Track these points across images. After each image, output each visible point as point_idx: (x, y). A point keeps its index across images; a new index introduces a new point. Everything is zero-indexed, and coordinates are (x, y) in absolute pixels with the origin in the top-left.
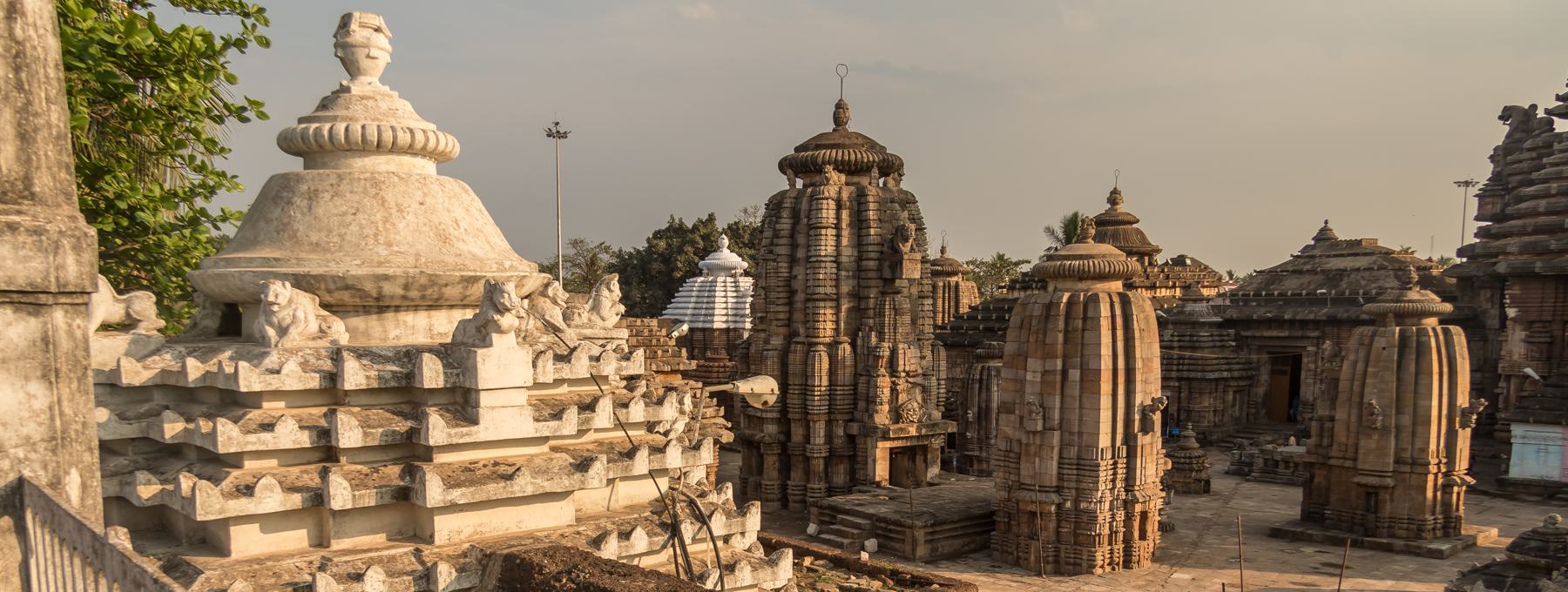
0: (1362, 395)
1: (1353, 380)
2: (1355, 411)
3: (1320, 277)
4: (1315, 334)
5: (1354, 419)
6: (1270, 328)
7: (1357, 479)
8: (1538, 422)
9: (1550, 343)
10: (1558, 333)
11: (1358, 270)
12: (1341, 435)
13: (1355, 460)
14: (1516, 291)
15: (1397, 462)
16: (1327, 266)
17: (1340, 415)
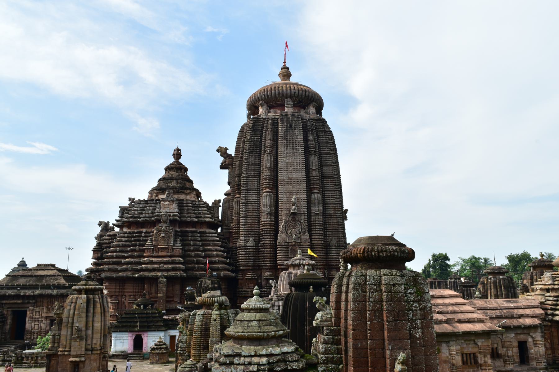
0: (73, 323)
1: (69, 317)
2: (69, 330)
3: (34, 278)
4: (34, 301)
5: (69, 333)
6: (13, 299)
7: (71, 359)
8: (120, 331)
9: (118, 303)
10: (120, 299)
11: (49, 276)
12: (63, 342)
13: (69, 351)
14: (107, 284)
15: (86, 350)
16: (37, 274)
17: (63, 332)
